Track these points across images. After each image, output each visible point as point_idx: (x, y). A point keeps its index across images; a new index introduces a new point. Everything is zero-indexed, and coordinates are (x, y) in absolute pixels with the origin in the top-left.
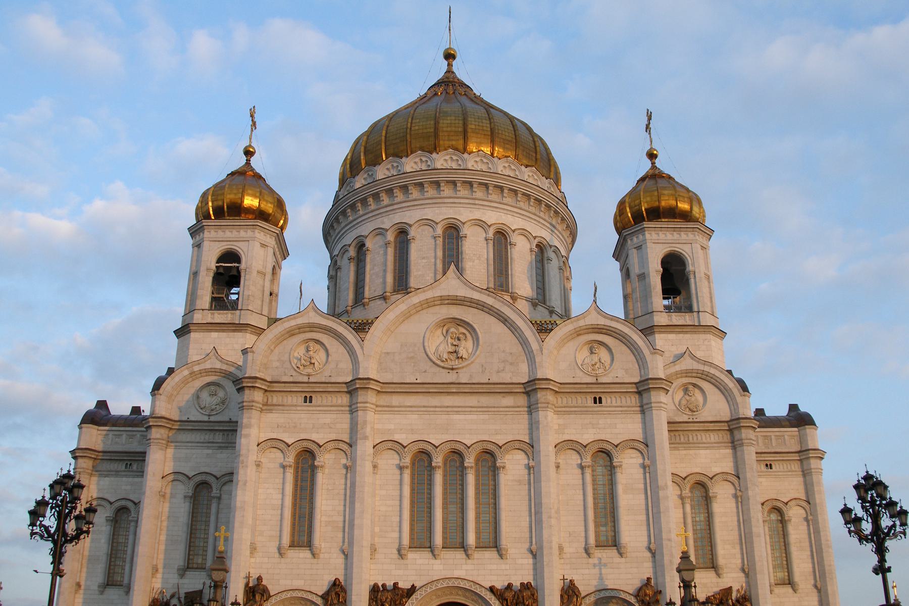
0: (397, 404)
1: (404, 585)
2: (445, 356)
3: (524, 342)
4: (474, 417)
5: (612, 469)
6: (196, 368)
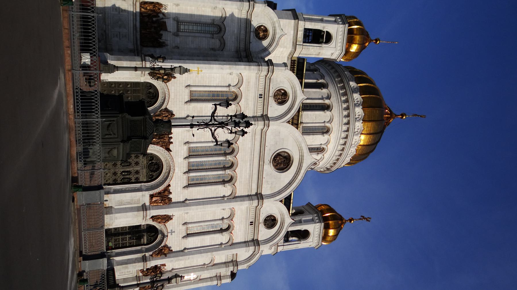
1: (171, 147)
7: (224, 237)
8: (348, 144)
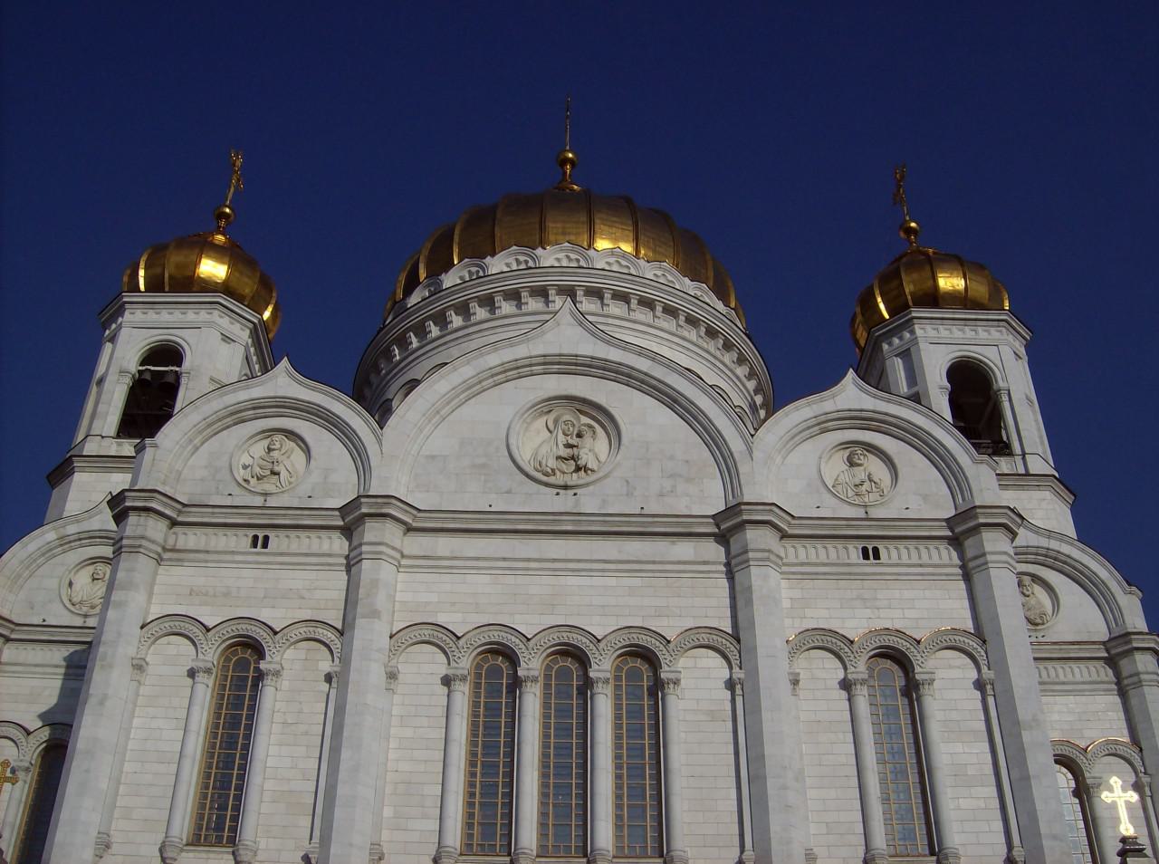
0: (447, 554)
2: (552, 463)
3: (713, 439)
4: (612, 582)
5: (912, 689)
6: (72, 529)
7: (940, 674)
8: (624, 287)
